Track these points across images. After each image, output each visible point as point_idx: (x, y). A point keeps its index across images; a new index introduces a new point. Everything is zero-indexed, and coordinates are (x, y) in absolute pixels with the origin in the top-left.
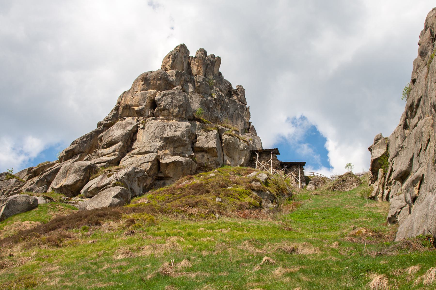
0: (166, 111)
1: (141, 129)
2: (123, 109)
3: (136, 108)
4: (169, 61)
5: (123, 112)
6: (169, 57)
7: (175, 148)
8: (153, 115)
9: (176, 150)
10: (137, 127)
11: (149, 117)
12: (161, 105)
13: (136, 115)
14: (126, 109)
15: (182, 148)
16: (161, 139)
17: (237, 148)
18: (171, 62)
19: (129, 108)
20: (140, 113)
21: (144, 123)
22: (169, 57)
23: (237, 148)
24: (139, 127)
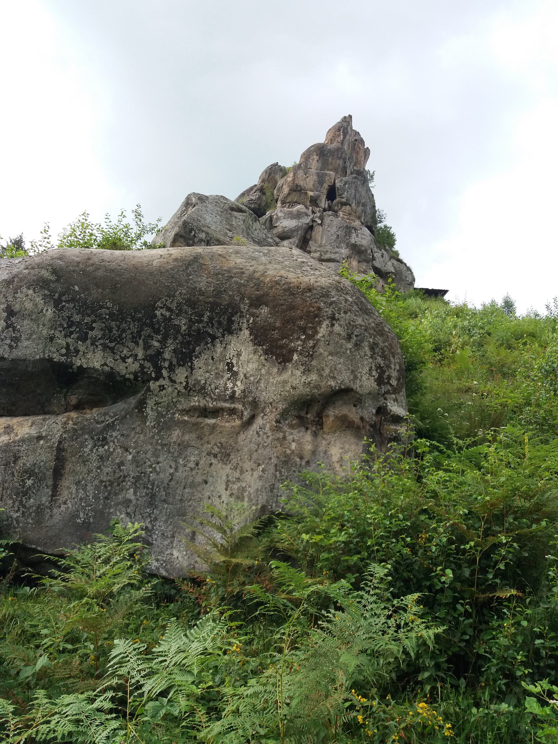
0: (348, 206)
1: (319, 224)
2: (290, 190)
3: (311, 194)
4: (339, 136)
5: (289, 194)
6: (339, 130)
7: (359, 262)
8: (330, 208)
9: (360, 264)
10: (313, 221)
11: (325, 210)
12: (344, 196)
13: (308, 203)
14: (294, 191)
15: (365, 264)
16: (347, 245)
17: (403, 280)
18: (342, 136)
19: (300, 191)
20: (314, 202)
21: (321, 218)
22: (339, 130)
23: (403, 280)
24: (313, 221)
